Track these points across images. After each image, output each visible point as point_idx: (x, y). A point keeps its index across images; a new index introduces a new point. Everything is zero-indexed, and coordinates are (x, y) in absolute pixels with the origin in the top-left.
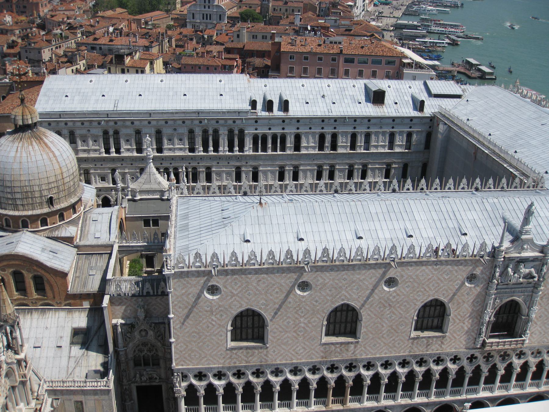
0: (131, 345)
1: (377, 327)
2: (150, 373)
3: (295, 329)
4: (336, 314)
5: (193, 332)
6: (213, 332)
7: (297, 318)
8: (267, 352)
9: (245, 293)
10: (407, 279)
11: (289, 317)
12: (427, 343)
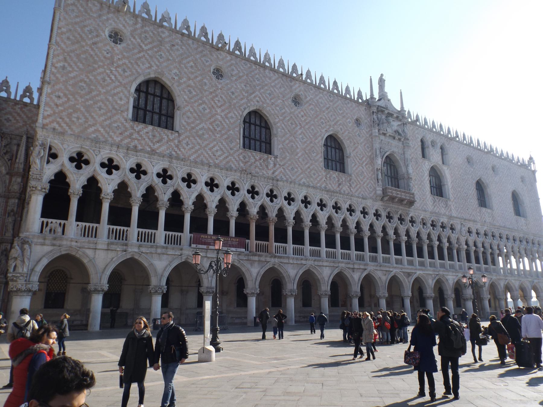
1: (292, 146)
3: (212, 120)
4: (250, 126)
5: (81, 81)
6: (111, 90)
7: (212, 106)
8: (179, 142)
9: (156, 52)
10: (310, 100)
11: (204, 102)
12: (338, 181)
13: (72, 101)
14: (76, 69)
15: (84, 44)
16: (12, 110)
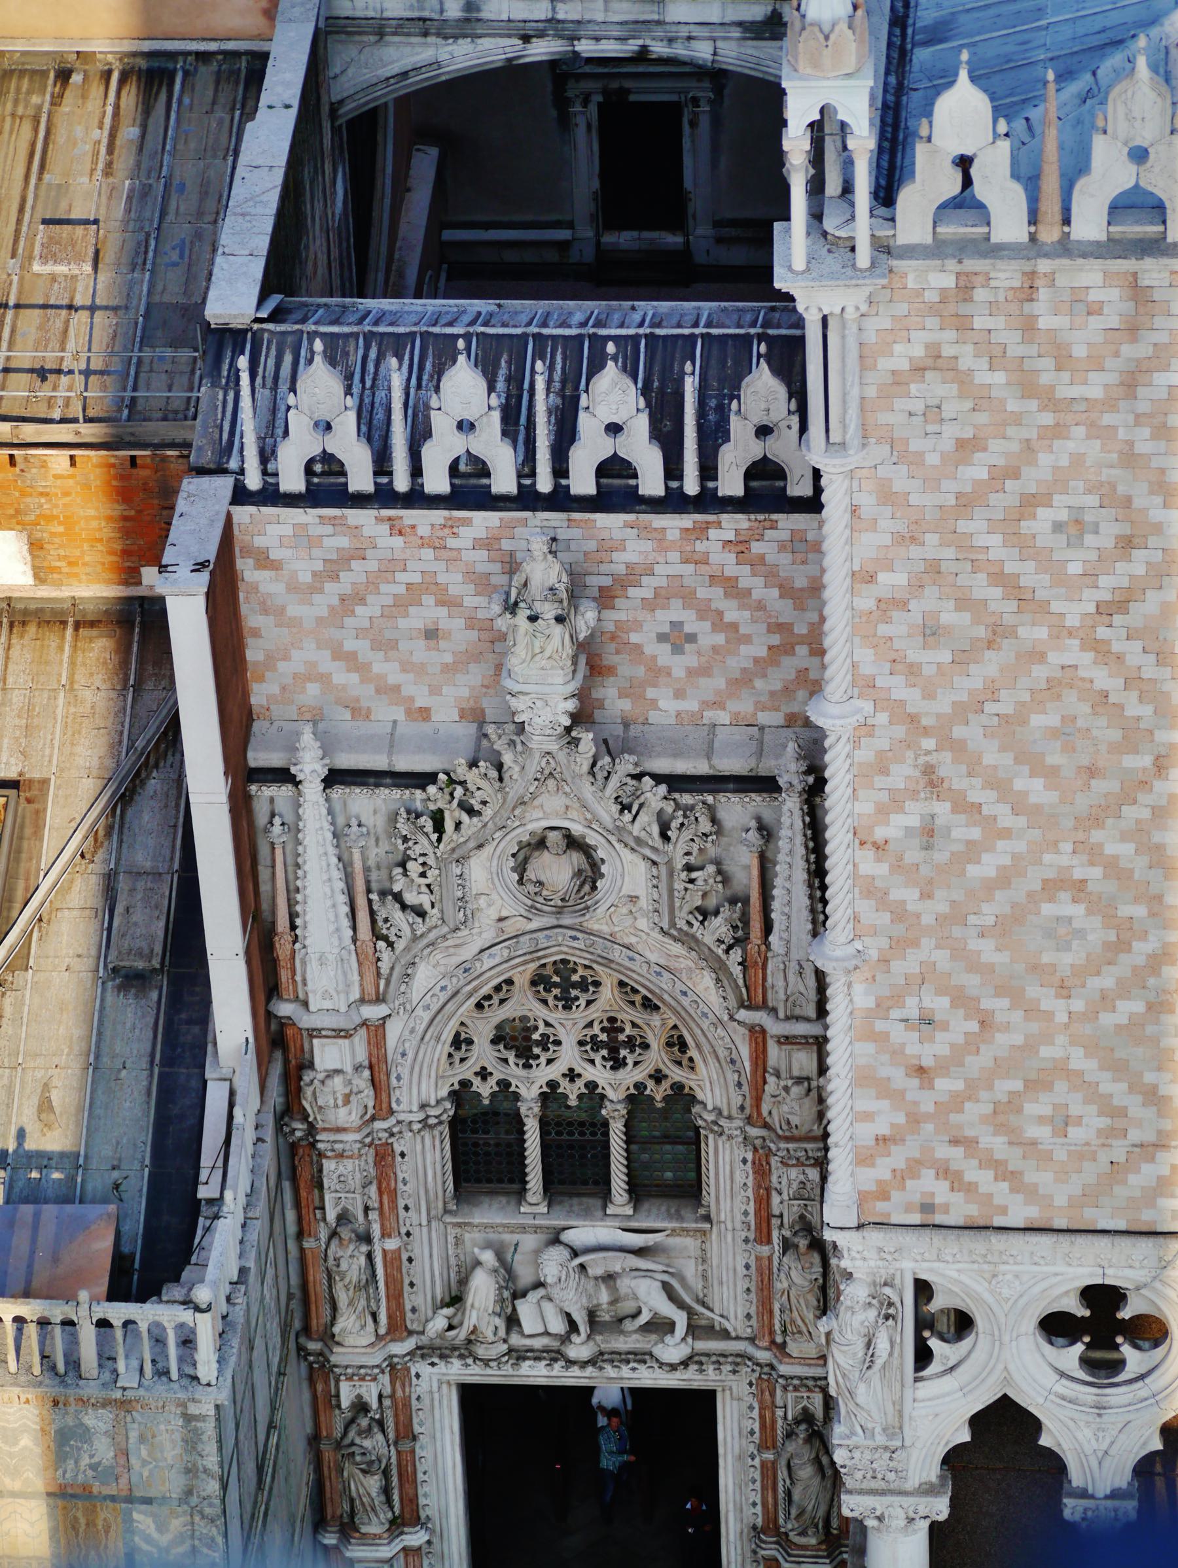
0: (425, 976)
2: (598, 1265)
5: (1051, 888)
13: (1007, 1027)
14: (1006, 818)
15: (1042, 633)
16: (690, 568)
